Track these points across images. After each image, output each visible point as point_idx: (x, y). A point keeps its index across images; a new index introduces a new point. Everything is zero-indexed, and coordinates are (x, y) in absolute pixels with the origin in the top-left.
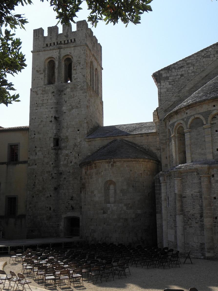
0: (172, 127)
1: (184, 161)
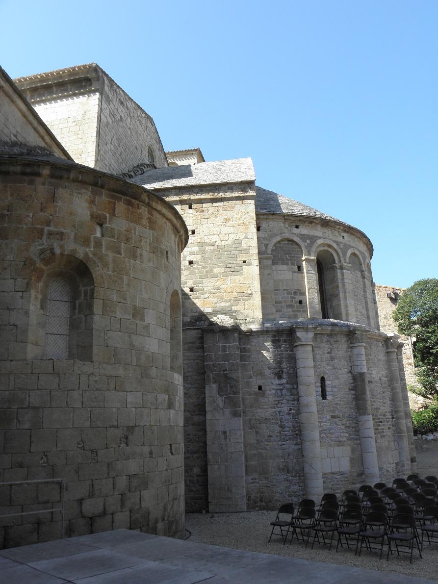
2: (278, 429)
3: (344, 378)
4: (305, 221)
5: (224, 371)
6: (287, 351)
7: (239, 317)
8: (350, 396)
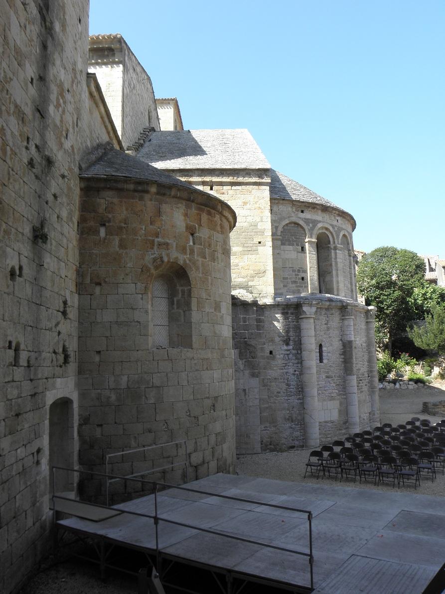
0: (311, 225)
2: (284, 386)
3: (337, 344)
4: (309, 207)
5: (244, 339)
6: (293, 322)
7: (255, 291)
8: (341, 360)
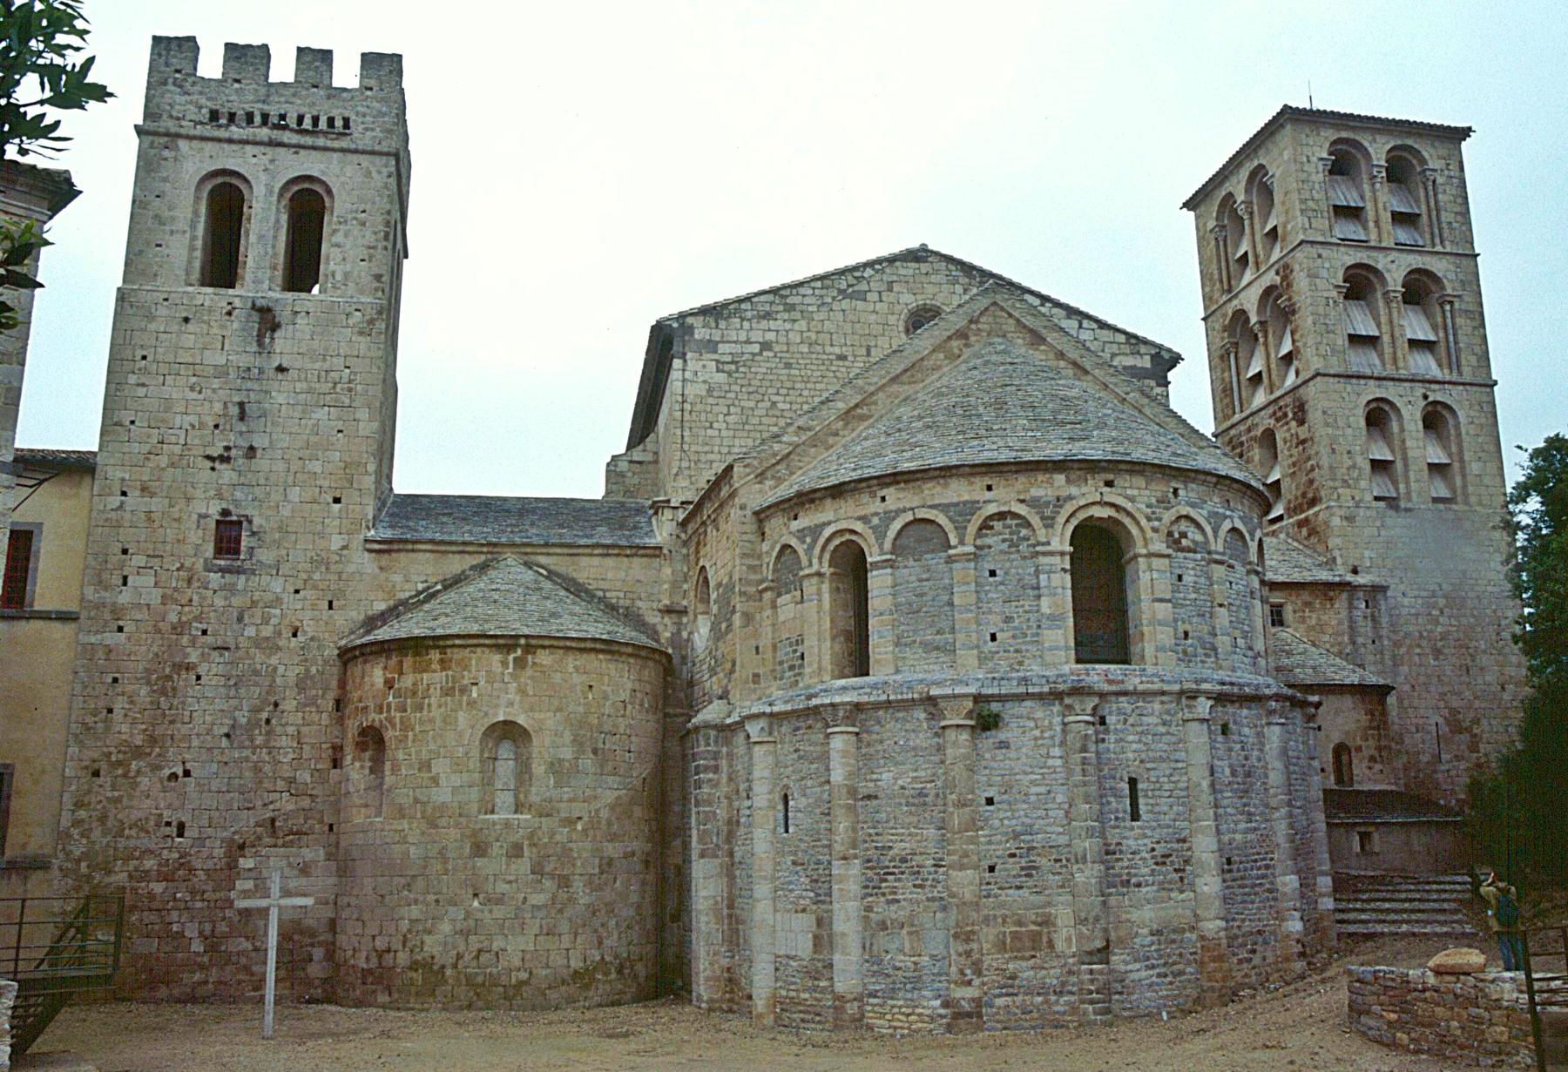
0: (808, 540)
1: (860, 664)
